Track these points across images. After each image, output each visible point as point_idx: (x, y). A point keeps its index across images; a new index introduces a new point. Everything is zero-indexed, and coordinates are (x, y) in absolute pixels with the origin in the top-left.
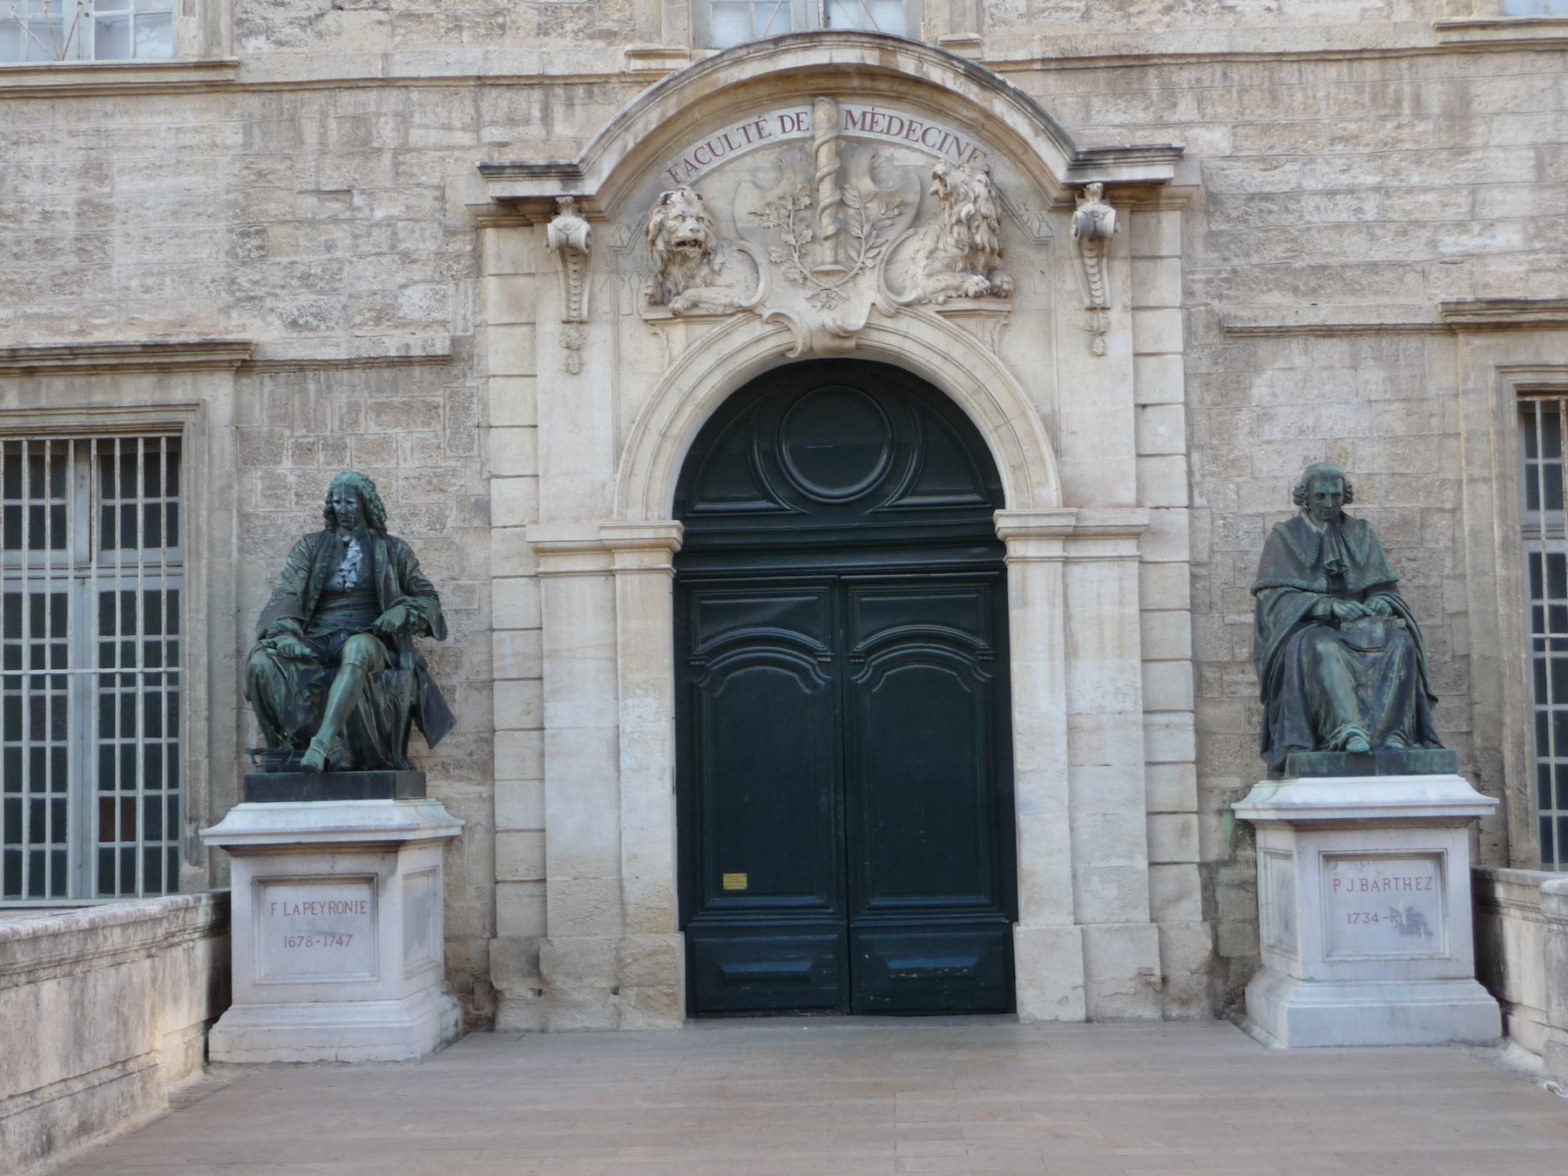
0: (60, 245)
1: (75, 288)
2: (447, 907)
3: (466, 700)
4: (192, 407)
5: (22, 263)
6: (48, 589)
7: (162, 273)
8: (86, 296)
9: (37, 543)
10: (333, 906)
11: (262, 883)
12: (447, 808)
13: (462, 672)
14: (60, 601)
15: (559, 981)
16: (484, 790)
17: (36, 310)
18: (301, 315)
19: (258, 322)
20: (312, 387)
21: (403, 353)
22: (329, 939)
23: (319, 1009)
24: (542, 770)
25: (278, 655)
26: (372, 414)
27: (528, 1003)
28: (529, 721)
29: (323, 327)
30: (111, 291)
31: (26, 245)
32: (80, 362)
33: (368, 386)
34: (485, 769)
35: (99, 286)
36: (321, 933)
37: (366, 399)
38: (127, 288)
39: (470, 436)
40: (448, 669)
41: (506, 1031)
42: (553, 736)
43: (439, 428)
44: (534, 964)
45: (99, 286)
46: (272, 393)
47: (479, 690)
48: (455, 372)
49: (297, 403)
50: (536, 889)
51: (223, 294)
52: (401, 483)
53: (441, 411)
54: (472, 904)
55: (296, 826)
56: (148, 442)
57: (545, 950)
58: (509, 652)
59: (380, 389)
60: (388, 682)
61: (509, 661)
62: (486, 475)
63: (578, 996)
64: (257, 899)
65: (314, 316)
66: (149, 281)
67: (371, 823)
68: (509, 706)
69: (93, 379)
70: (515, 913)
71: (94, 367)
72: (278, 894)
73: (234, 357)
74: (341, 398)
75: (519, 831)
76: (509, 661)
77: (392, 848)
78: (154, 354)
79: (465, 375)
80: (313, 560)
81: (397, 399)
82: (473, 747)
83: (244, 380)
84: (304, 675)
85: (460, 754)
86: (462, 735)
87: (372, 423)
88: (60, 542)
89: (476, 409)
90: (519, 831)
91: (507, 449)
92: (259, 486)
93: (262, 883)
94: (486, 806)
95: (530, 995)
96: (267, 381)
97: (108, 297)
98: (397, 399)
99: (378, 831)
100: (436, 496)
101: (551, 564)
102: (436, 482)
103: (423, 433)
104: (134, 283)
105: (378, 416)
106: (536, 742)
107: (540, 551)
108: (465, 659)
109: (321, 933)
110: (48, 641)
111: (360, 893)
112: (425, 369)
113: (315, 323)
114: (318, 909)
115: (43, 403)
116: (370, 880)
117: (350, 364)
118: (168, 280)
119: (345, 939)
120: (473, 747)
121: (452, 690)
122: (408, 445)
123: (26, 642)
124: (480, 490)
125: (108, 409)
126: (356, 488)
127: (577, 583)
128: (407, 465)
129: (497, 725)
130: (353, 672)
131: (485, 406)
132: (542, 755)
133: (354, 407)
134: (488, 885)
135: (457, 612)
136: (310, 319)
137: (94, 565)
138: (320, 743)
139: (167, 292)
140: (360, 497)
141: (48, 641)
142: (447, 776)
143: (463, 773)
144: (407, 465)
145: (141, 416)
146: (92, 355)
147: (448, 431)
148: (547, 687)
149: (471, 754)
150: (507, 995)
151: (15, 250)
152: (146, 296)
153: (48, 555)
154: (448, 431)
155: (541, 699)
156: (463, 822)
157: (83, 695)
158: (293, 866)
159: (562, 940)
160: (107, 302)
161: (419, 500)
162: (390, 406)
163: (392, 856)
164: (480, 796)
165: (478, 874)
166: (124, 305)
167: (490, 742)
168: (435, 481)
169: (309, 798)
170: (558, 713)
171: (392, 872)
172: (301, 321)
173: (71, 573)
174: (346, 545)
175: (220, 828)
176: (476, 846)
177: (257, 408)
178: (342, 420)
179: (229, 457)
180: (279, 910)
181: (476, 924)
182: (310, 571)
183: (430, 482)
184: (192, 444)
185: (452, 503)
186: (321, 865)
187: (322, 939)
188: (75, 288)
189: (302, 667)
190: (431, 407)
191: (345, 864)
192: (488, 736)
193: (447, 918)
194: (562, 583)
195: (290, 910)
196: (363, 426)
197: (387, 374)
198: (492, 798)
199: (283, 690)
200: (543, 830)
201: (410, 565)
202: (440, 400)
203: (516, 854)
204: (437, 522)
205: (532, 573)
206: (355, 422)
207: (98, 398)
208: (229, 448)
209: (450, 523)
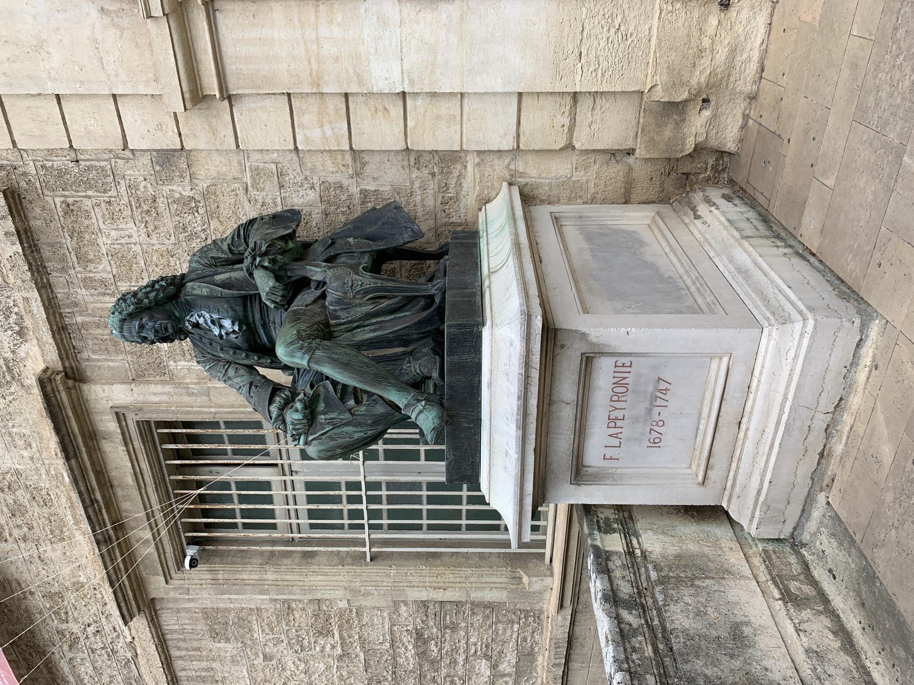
0: (12, 501)
1: (44, 492)
2: (593, 201)
3: (375, 179)
4: (120, 417)
5: (35, 525)
6: (301, 493)
7: (10, 434)
8: (48, 486)
9: (269, 500)
10: (616, 397)
11: (579, 473)
12: (488, 201)
13: (346, 183)
14: (309, 486)
15: (699, 78)
16: (472, 160)
17: (69, 517)
18: (11, 328)
19: (29, 363)
20: (79, 319)
21: (15, 238)
22: (659, 402)
23: (753, 425)
24: (452, 94)
25: (307, 434)
26: (91, 267)
27: (715, 116)
28: (396, 110)
29: (16, 310)
30: (37, 469)
31: (19, 522)
32: (98, 496)
33: (64, 270)
34: (448, 160)
35: (36, 477)
36: (649, 411)
37: (77, 272)
38: (32, 458)
39: (89, 169)
40: (343, 198)
41: (741, 141)
42: (412, 83)
43: (88, 203)
44: (674, 110)
45: (36, 477)
46: (94, 352)
47: (364, 164)
48: (23, 184)
49: (99, 331)
50: (585, 105)
51: (12, 390)
52: (154, 241)
53: (70, 200)
54: (593, 176)
55: (514, 455)
56: (163, 442)
57: (660, 95)
58: (320, 131)
59: (63, 259)
60: (339, 302)
61: (329, 132)
62: (128, 153)
63: (721, 55)
64: (598, 478)
65: (7, 317)
66: (20, 443)
67: (515, 368)
68: (379, 132)
69: (115, 483)
70: (609, 127)
71: (101, 485)
72: (594, 456)
73: (61, 388)
74: (82, 294)
75: (519, 122)
76: (329, 132)
77: (551, 336)
78: (76, 448)
79: (25, 174)
80: (217, 359)
81: (69, 243)
82: (425, 172)
83: (89, 374)
84: (329, 407)
85: (432, 186)
86: (412, 183)
87: (101, 267)
88: (267, 485)
89: (57, 163)
90: (519, 122)
91: (93, 129)
92: (183, 363)
93: (579, 473)
94: (489, 158)
95: (706, 113)
96: (85, 355)
97: (43, 471)
98: (69, 243)
99: (527, 365)
100: (162, 205)
101: (211, 85)
102: (146, 209)
103: (97, 219)
104: (26, 454)
105: (90, 261)
106: (419, 102)
107: (196, 97)
108: (331, 179)
109: (649, 411)
110: (344, 493)
111: (604, 374)
112: (30, 216)
113: (15, 317)
114: (619, 413)
115: (142, 514)
116: (588, 361)
117: (45, 288)
118: (14, 430)
119: (663, 386)
120: (425, 172)
121: (365, 193)
122: (114, 234)
123: (346, 507)
124: (145, 160)
125: (138, 475)
126: (123, 321)
127: (229, 50)
128: (135, 235)
129: (401, 146)
130: (318, 362)
131: (51, 151)
132: (434, 95)
133: (88, 283)
134: (575, 158)
135: (281, 187)
136: (11, 320)
137: (279, 462)
138: (407, 406)
139: (26, 431)
140: (131, 316)
141: (344, 493)
142: (457, 199)
143: (452, 182)
144: (135, 235)
145: (138, 452)
146: (90, 491)
147: (90, 193)
148: (353, 88)
149: (433, 175)
150: (700, 139)
151: (25, 529)
152: (34, 445)
153: (276, 492)
154: (90, 193)
155: (370, 95)
156: (505, 184)
157: (386, 472)
158: (562, 444)
159: (650, 76)
160: (48, 472)
161: (168, 223)
162: (78, 250)
163: (560, 336)
164: (478, 165)
165: (560, 168)
166: (47, 462)
167: (419, 154)
168: (146, 208)
169: (478, 422)
170: (385, 76)
171: (584, 336)
172: (17, 328)
173: (288, 478)
174: (197, 325)
175: (509, 517)
176: (534, 171)
177: (110, 364)
178: (104, 294)
179: (159, 388)
180: (610, 453)
181: (615, 171)
182: (229, 363)
183: (148, 212)
184: (155, 416)
185: (166, 189)
186: (566, 415)
187: (656, 410)
188: (44, 492)
189: (322, 406)
190: (69, 209)
191: (567, 390)
192: (412, 156)
193: (604, 201)
194: (231, 68)
195: (616, 442)
196: (104, 275)
197: (46, 252)
198: (480, 153)
199: (349, 429)
200: (520, 95)
201: (215, 254)
202: (58, 200)
203: (544, 126)
204: (188, 205)
205: (226, 103)
206: (103, 282)
207: (130, 480)
208: (153, 388)
209: (187, 193)
